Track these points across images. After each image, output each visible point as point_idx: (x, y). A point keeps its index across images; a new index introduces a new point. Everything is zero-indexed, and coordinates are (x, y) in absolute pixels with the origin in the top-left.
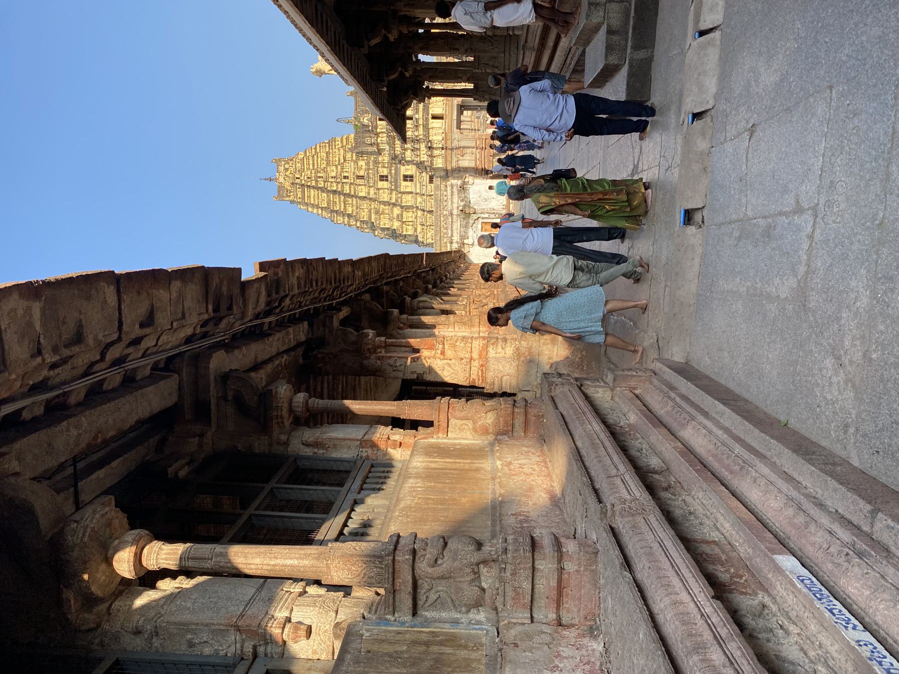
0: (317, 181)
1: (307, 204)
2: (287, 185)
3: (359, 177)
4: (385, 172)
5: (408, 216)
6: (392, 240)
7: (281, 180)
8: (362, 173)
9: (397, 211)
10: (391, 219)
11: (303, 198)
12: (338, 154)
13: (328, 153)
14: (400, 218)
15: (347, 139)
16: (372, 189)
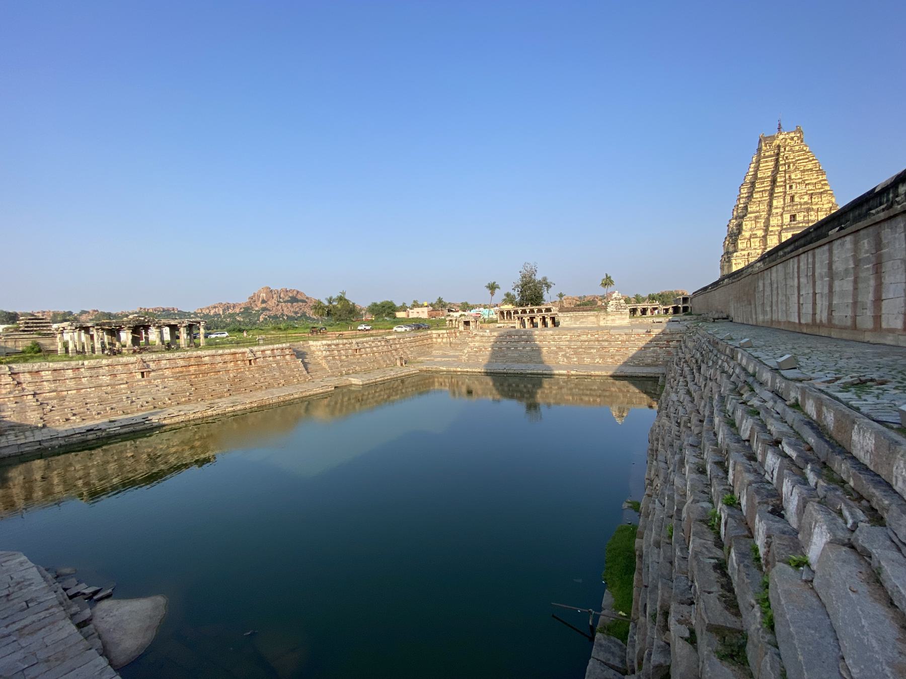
0: (785, 164)
1: (758, 162)
2: (777, 142)
3: (792, 198)
4: (800, 217)
5: (756, 243)
6: (726, 234)
7: (781, 137)
8: (797, 199)
9: (760, 233)
10: (751, 230)
11: (765, 157)
12: (812, 178)
13: (811, 170)
14: (753, 236)
15: (825, 184)
16: (781, 210)
